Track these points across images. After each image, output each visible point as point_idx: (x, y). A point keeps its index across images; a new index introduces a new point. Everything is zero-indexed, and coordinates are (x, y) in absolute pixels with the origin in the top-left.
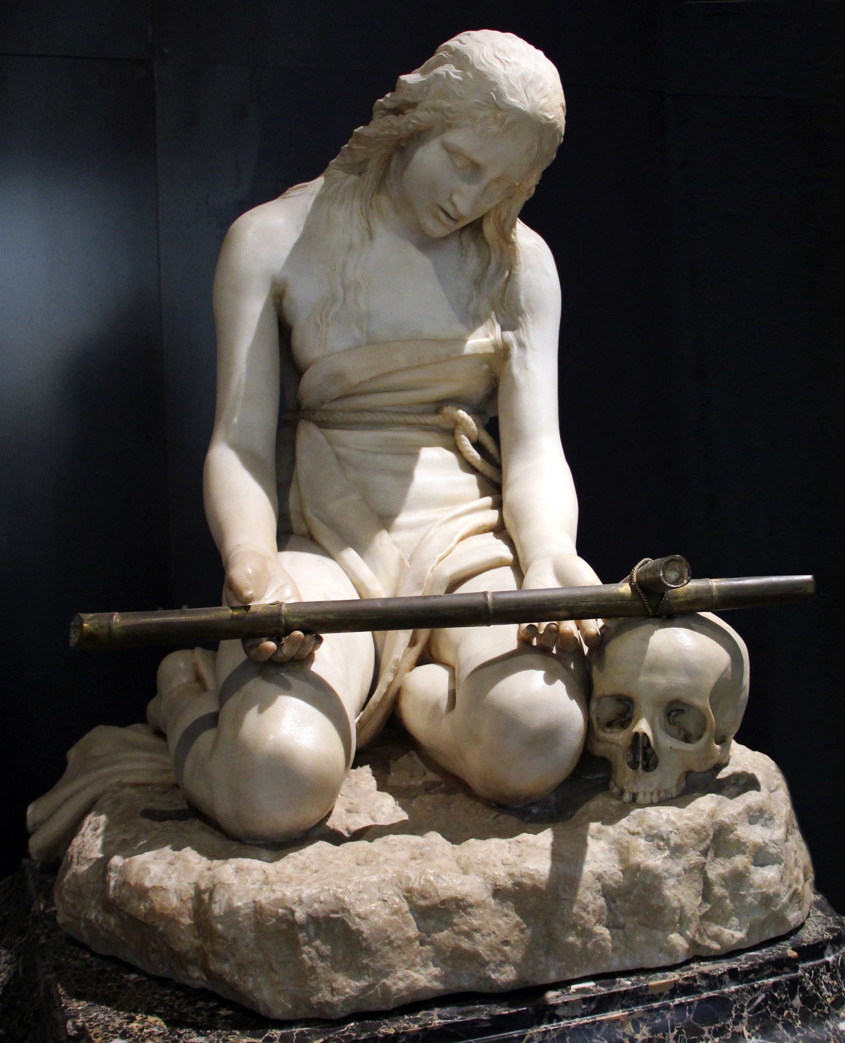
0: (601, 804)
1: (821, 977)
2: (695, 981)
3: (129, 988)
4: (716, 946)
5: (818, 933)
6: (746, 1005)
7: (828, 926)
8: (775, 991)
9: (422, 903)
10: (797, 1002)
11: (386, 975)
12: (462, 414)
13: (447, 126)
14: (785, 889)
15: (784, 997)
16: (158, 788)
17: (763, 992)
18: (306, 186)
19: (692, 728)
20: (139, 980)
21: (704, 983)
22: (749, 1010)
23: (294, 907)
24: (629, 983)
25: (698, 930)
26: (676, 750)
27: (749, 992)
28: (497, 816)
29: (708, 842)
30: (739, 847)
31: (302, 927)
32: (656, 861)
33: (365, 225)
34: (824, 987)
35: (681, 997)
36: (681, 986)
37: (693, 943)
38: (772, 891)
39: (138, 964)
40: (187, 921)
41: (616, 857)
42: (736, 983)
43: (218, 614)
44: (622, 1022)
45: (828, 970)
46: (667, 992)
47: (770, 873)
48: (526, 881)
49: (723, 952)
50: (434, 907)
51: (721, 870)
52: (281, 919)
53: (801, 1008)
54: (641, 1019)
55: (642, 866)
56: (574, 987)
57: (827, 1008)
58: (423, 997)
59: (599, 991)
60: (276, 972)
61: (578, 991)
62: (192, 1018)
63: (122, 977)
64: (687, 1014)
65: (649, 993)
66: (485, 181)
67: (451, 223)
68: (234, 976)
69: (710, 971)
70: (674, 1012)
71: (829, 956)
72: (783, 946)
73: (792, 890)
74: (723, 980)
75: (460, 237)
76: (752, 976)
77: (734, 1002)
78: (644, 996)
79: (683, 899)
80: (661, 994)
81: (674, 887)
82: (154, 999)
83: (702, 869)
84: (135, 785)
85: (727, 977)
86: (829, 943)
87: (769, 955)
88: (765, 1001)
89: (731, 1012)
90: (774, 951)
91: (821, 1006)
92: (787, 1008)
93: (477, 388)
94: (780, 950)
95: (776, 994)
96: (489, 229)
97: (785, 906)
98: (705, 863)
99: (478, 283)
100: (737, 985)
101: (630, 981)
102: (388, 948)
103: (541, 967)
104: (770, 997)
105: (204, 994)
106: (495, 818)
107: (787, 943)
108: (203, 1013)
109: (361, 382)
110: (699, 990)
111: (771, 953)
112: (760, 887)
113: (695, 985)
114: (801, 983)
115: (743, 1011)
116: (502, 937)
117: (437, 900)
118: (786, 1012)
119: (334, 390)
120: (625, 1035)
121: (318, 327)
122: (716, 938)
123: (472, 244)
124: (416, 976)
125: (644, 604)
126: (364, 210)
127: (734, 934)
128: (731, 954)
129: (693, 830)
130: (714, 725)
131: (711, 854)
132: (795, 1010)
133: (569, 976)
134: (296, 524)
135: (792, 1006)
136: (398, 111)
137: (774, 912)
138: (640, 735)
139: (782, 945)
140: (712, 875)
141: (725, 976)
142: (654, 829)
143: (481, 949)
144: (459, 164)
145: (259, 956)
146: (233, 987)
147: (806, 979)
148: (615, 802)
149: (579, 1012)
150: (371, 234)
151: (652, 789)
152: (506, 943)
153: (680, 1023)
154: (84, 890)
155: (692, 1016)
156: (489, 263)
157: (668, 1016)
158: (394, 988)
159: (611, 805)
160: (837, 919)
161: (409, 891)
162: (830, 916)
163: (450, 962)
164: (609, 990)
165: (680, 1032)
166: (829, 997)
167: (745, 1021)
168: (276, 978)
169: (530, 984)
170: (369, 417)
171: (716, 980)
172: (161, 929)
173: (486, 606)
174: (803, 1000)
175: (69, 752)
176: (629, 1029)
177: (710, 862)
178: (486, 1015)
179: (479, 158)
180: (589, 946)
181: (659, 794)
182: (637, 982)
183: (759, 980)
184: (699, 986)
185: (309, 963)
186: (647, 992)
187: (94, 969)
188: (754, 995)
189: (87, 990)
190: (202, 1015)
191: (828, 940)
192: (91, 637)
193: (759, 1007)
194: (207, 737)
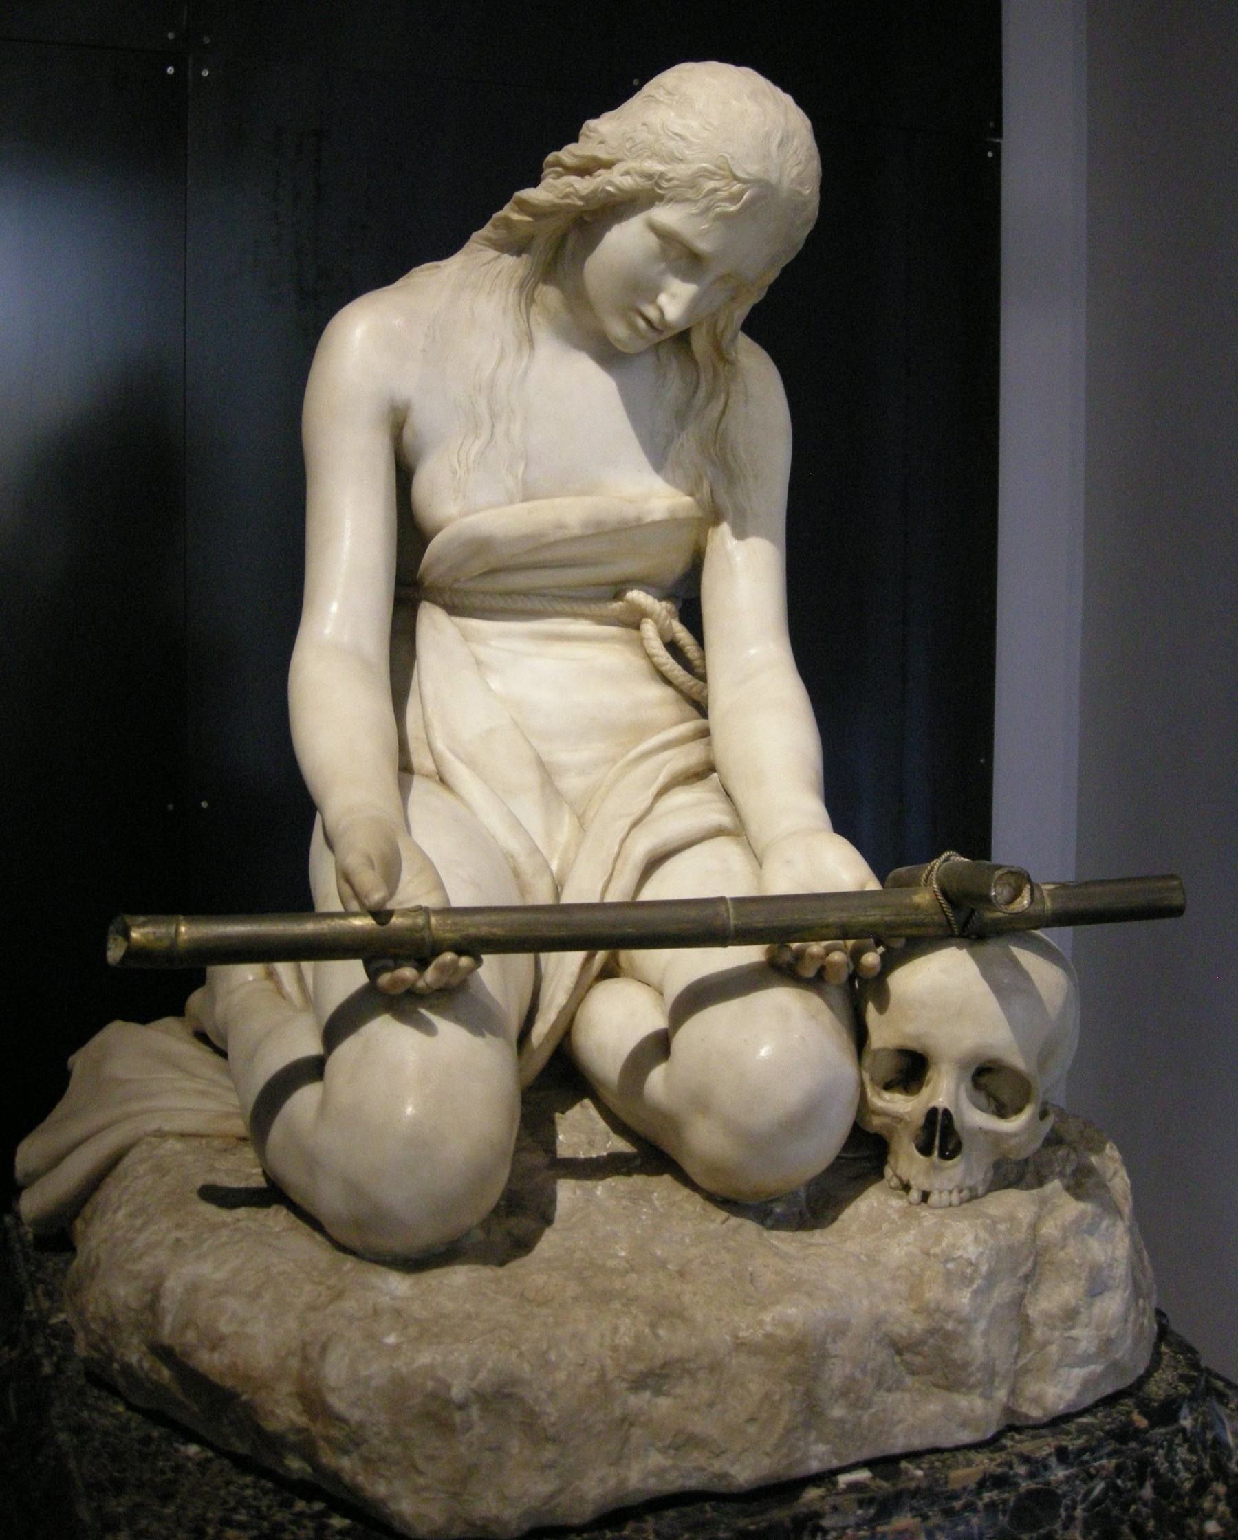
0: (875, 1205)
1: (1176, 1451)
2: (1011, 1467)
3: (189, 1473)
4: (1036, 1413)
5: (1170, 1384)
6: (1079, 1498)
7: (1180, 1371)
8: (1118, 1477)
10: (1147, 1492)
15: (1129, 1484)
16: (216, 1143)
17: (1103, 1479)
18: (439, 267)
19: (1005, 1096)
20: (203, 1456)
21: (1022, 1470)
22: (1084, 1506)
23: (449, 1379)
24: (920, 1473)
26: (986, 1132)
27: (1084, 1482)
28: (727, 1219)
29: (1030, 1264)
31: (462, 1407)
34: (1179, 1465)
35: (991, 1491)
36: (992, 1476)
38: (1113, 1333)
39: (203, 1432)
40: (285, 1388)
42: (1064, 1467)
43: (333, 923)
44: (912, 1533)
45: (1186, 1440)
46: (972, 1486)
48: (780, 1332)
49: (1045, 1420)
52: (434, 1396)
53: (1154, 1502)
55: (942, 1307)
56: (844, 1479)
57: (1187, 1499)
59: (879, 1488)
60: (421, 1473)
61: (854, 1487)
62: (293, 1533)
63: (177, 1451)
64: (1001, 1517)
65: (950, 1487)
68: (358, 1474)
69: (1032, 1451)
70: (982, 1514)
71: (1185, 1418)
72: (1124, 1408)
74: (1050, 1463)
76: (1086, 1457)
77: (1065, 1495)
78: (942, 1493)
80: (965, 1489)
82: (230, 1493)
83: (1018, 1303)
84: (183, 1136)
85: (1053, 1461)
86: (1186, 1401)
87: (1109, 1424)
88: (1105, 1492)
89: (1058, 1511)
90: (1115, 1415)
91: (1180, 1497)
92: (1134, 1501)
94: (1122, 1414)
95: (1119, 1482)
98: (1023, 1296)
100: (1067, 1469)
101: (921, 1468)
103: (798, 1455)
104: (1111, 1486)
105: (308, 1490)
106: (723, 1222)
107: (1129, 1402)
108: (306, 1522)
110: (1016, 1479)
111: (1109, 1420)
113: (1011, 1473)
114: (1154, 1464)
115: (1074, 1509)
118: (1133, 1508)
122: (1037, 1400)
123: (674, 361)
125: (946, 916)
128: (1057, 1422)
132: (1145, 1504)
133: (835, 1463)
134: (420, 759)
135: (1140, 1498)
138: (940, 1111)
139: (1123, 1405)
140: (1033, 1312)
141: (1051, 1459)
142: (958, 1249)
145: (396, 1450)
146: (354, 1490)
147: (1159, 1457)
148: (896, 1203)
149: (852, 1521)
151: (950, 1188)
152: (752, 1420)
153: (991, 1531)
154: (121, 1319)
155: (1006, 1519)
157: (975, 1520)
159: (892, 1207)
160: (1190, 1359)
161: (615, 1349)
162: (1180, 1353)
163: (672, 1452)
164: (894, 1485)
166: (1187, 1479)
167: (1079, 1523)
168: (421, 1481)
169: (784, 1479)
171: (1039, 1465)
172: (244, 1397)
174: (1155, 1488)
175: (71, 1059)
177: (1031, 1293)
178: (726, 1530)
180: (866, 1418)
181: (960, 1191)
182: (932, 1471)
183: (1095, 1460)
184: (1016, 1475)
186: (946, 1487)
187: (134, 1434)
188: (1091, 1484)
189: (128, 1475)
190: (305, 1527)
191: (1184, 1397)
192: (135, 953)
193: (1097, 1502)
194: (305, 1098)
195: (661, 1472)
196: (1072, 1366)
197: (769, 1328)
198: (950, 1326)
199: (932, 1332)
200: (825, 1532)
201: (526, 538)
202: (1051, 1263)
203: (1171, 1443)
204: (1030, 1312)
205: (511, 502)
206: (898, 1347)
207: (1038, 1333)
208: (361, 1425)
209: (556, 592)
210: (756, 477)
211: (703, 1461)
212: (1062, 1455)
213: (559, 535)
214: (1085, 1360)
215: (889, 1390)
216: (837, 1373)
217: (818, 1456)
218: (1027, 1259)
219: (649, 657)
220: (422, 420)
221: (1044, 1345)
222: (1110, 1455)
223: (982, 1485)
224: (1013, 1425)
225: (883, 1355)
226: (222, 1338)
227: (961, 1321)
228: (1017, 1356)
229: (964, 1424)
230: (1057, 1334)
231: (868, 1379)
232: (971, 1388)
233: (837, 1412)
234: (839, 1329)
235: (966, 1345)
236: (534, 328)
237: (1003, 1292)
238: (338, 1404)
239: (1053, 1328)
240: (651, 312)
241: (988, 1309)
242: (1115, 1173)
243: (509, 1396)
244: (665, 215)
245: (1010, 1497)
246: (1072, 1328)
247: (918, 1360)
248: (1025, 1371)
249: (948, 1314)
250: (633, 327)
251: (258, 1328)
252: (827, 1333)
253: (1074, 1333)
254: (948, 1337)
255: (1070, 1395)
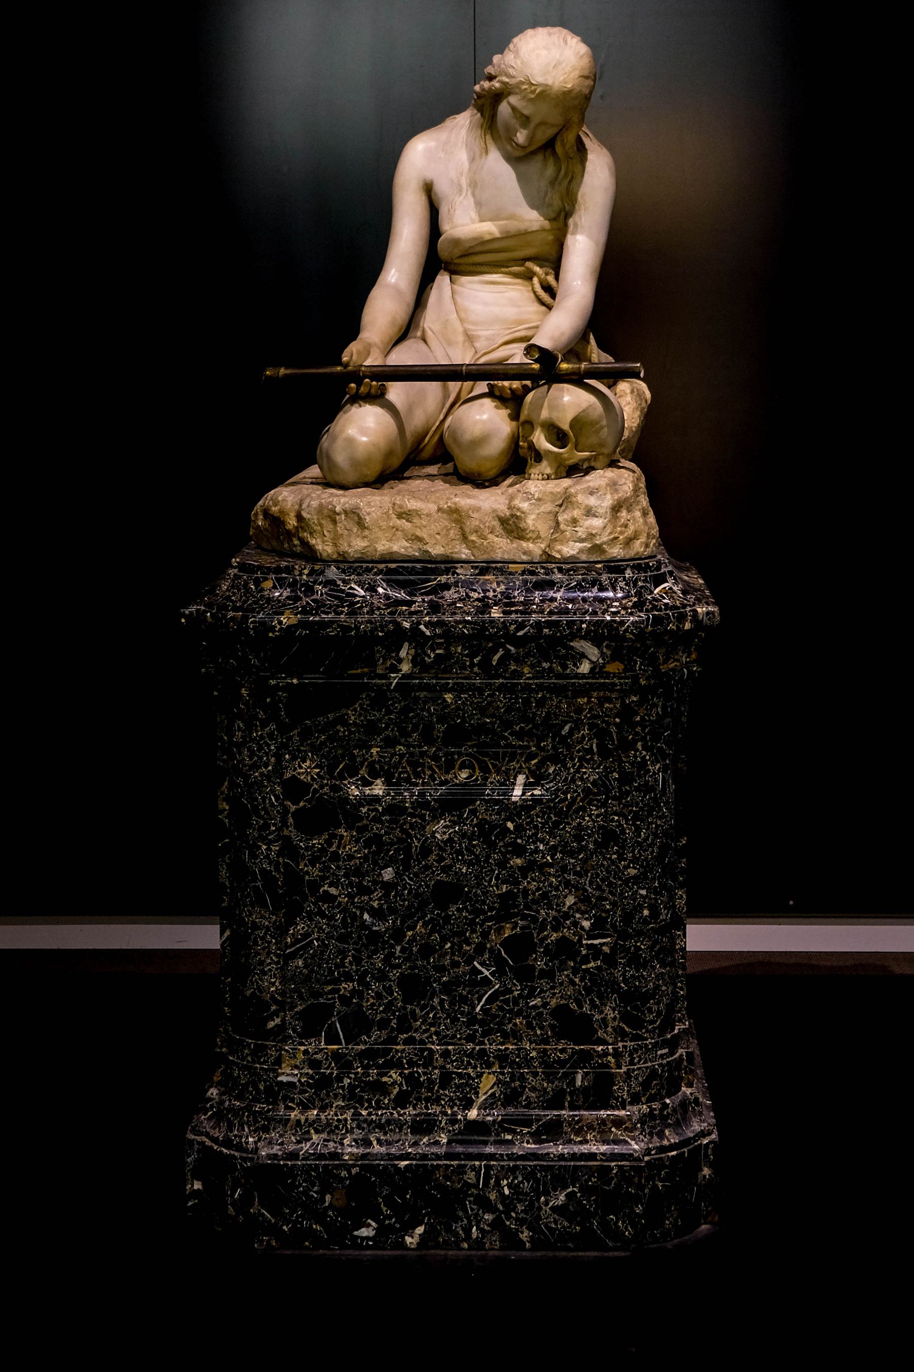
2: (537, 569)
4: (558, 556)
9: (399, 510)
11: (376, 543)
12: (537, 269)
13: (509, 94)
14: (607, 534)
21: (542, 571)
25: (549, 546)
29: (561, 501)
30: (578, 505)
31: (338, 514)
32: (525, 506)
33: (483, 145)
37: (544, 552)
38: (594, 532)
40: (292, 514)
41: (507, 502)
47: (597, 523)
50: (404, 513)
51: (566, 517)
54: (502, 582)
58: (395, 557)
66: (532, 126)
67: (520, 149)
73: (612, 536)
75: (544, 154)
76: (571, 573)
79: (539, 528)
80: (517, 572)
81: (533, 520)
83: (556, 515)
85: (556, 570)
93: (549, 251)
96: (559, 149)
97: (605, 543)
99: (553, 182)
102: (377, 530)
109: (470, 247)
112: (587, 528)
116: (436, 532)
117: (406, 510)
119: (457, 252)
120: (491, 588)
121: (449, 211)
122: (559, 552)
124: (392, 545)
126: (483, 136)
127: (570, 549)
129: (551, 493)
130: (574, 440)
131: (563, 508)
136: (491, 78)
137: (596, 545)
140: (560, 519)
143: (425, 536)
144: (518, 115)
149: (469, 573)
150: (487, 153)
151: (538, 472)
152: (438, 534)
156: (560, 170)
158: (379, 549)
161: (394, 504)
165: (522, 591)
170: (480, 269)
173: (462, 370)
176: (494, 585)
179: (526, 112)
181: (543, 475)
184: (539, 572)
185: (340, 532)
195: (406, 548)
196: (575, 542)
197: (449, 504)
198: (518, 514)
199: (512, 515)
200: (458, 575)
201: (475, 239)
202: (570, 502)
203: (616, 580)
204: (559, 519)
205: (473, 223)
206: (503, 521)
207: (562, 527)
208: (309, 519)
209: (496, 263)
210: (585, 210)
211: (421, 547)
212: (560, 570)
213: (488, 237)
214: (581, 540)
215: (497, 536)
216: (473, 523)
217: (464, 553)
218: (560, 499)
219: (535, 292)
220: (442, 187)
221: (563, 532)
222: (582, 575)
223: (523, 573)
224: (548, 558)
225: (496, 523)
226: (279, 502)
227: (523, 513)
228: (553, 533)
229: (524, 553)
230: (569, 528)
231: (487, 529)
232: (528, 540)
233: (473, 538)
234: (478, 509)
235: (525, 522)
236: (488, 145)
237: (548, 507)
238: (304, 514)
239: (568, 526)
240: (516, 141)
241: (537, 512)
242: (625, 484)
243: (354, 513)
244: (513, 99)
245: (534, 578)
246: (575, 527)
247: (508, 527)
248: (555, 540)
249: (519, 509)
250: (512, 146)
251: (289, 499)
252: (470, 509)
253: (576, 529)
254: (517, 517)
255: (572, 552)
